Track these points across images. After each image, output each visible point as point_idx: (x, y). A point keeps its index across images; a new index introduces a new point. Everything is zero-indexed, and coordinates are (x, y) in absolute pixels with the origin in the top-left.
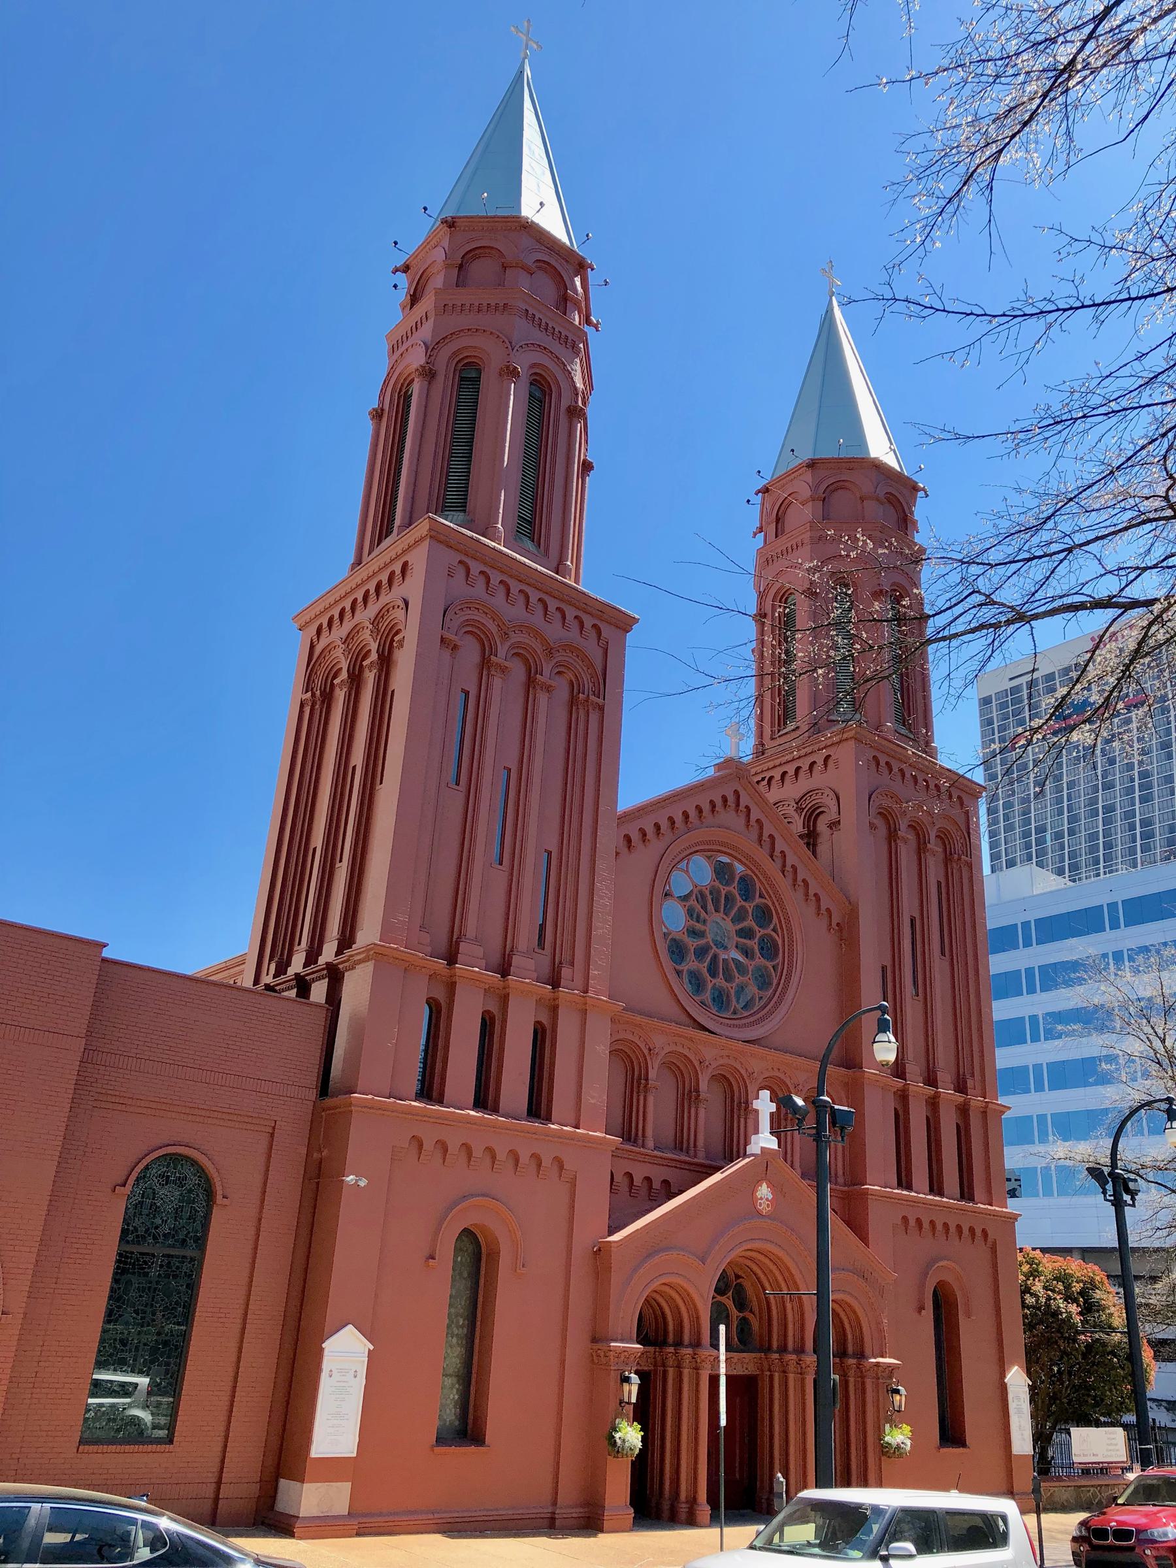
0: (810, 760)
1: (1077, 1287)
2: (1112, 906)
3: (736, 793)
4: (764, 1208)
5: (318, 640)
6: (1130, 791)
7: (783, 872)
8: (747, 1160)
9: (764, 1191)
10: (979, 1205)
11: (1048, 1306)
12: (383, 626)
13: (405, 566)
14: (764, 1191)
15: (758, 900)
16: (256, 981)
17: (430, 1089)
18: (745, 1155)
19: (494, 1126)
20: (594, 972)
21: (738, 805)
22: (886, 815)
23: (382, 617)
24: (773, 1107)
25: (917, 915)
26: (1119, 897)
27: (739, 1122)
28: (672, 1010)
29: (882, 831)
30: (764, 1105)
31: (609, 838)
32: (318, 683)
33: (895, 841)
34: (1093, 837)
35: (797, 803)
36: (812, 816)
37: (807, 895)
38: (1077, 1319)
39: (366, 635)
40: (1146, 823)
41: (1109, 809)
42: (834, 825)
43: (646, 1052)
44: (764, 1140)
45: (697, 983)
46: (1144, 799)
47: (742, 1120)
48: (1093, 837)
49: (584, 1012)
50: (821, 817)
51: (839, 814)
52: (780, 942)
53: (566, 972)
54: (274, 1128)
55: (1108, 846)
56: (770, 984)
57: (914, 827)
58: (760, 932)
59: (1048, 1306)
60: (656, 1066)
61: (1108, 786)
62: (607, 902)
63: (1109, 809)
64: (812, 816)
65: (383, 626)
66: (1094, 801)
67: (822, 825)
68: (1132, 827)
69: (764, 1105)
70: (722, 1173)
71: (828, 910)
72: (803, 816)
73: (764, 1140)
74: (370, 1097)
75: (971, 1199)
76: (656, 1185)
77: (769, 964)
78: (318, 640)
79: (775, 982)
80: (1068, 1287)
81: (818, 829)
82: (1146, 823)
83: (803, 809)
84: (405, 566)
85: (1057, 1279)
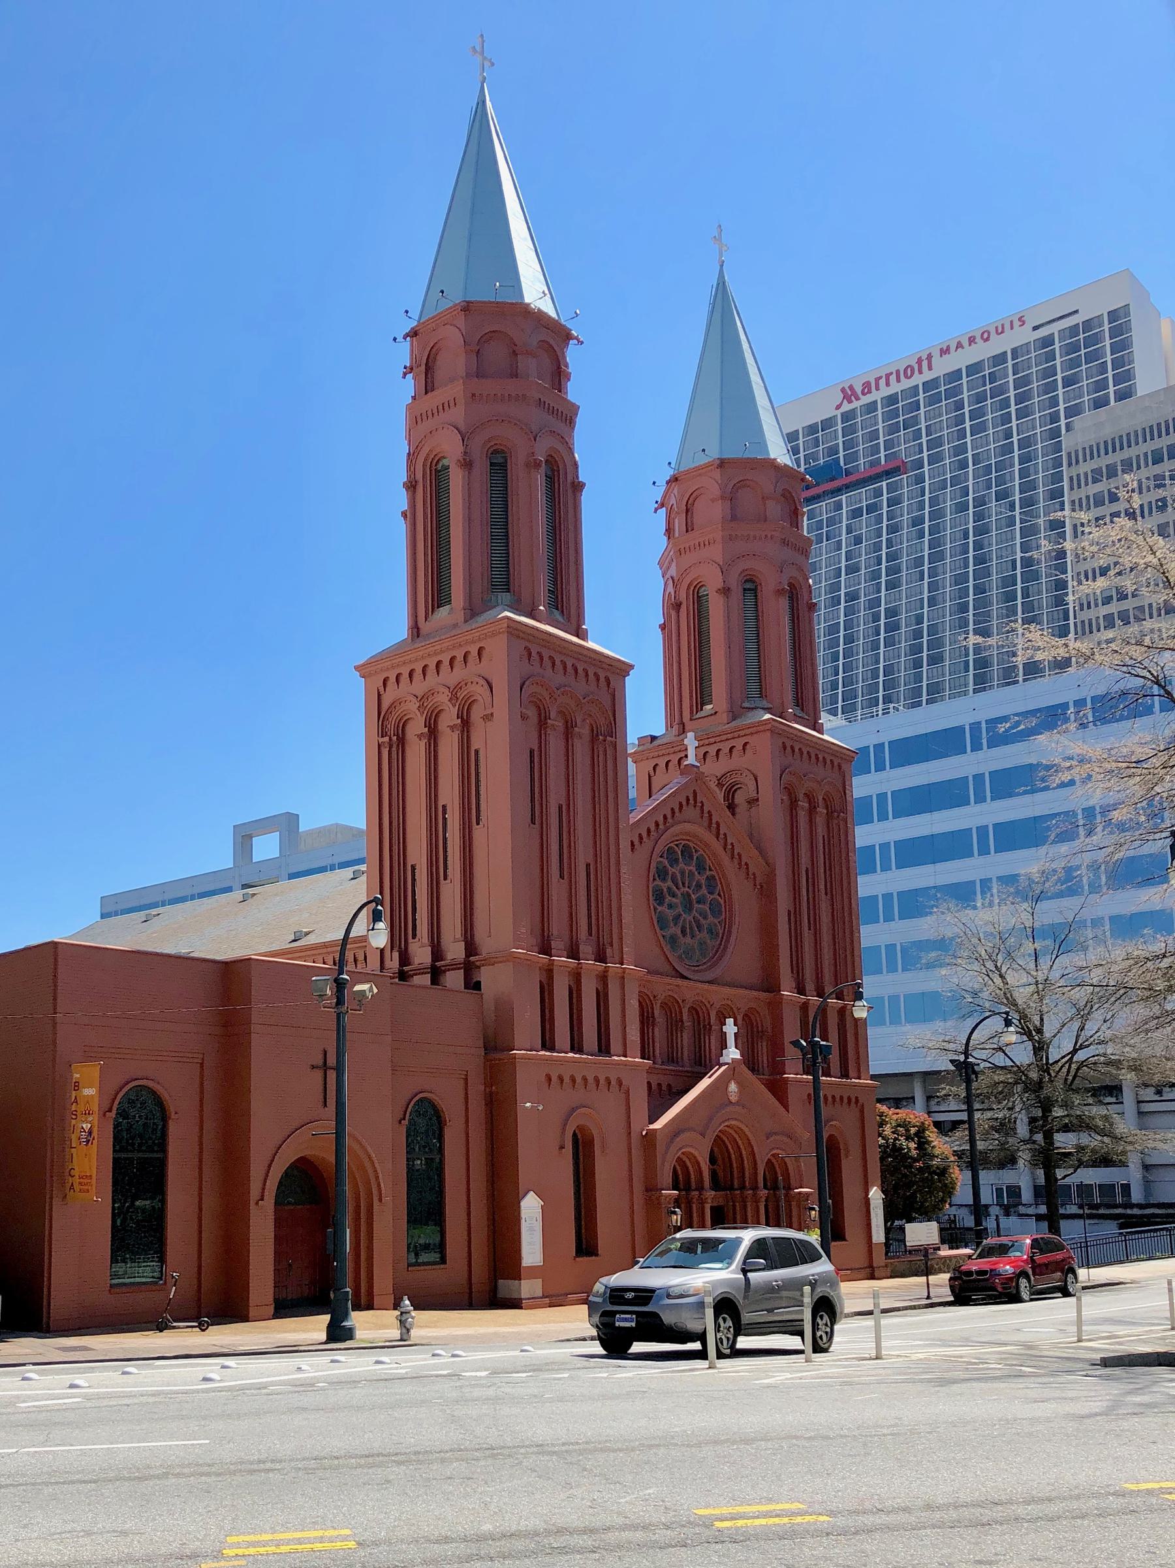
0: (729, 744)
1: (913, 1131)
2: (879, 747)
3: (695, 793)
4: (733, 1099)
5: (385, 690)
6: (876, 575)
7: (725, 849)
8: (723, 1068)
9: (733, 1087)
10: (853, 1080)
11: (894, 1144)
12: (461, 695)
13: (480, 651)
14: (733, 1087)
15: (708, 873)
16: (382, 967)
17: (548, 1043)
18: (721, 1065)
19: (585, 1062)
20: (625, 949)
21: (695, 802)
22: (790, 791)
23: (461, 688)
24: (735, 1029)
25: (810, 867)
26: (885, 738)
27: (704, 1038)
28: (667, 968)
29: (787, 802)
30: (730, 1028)
31: (624, 845)
32: (390, 727)
33: (795, 809)
34: (833, 629)
35: (718, 780)
36: (730, 793)
37: (740, 864)
38: (914, 1153)
39: (443, 698)
40: (892, 612)
41: (852, 597)
42: (752, 802)
43: (652, 998)
44: (733, 1053)
45: (673, 940)
46: (891, 585)
47: (707, 1037)
48: (833, 629)
49: (623, 978)
50: (738, 791)
51: (758, 793)
52: (722, 902)
53: (609, 951)
54: (467, 1075)
55: (849, 639)
56: (717, 934)
57: (809, 797)
58: (710, 897)
59: (894, 1144)
60: (658, 1005)
61: (852, 569)
62: (630, 897)
63: (852, 597)
64: (730, 793)
65: (461, 695)
66: (835, 587)
67: (740, 798)
68: (876, 618)
69: (730, 1028)
70: (710, 1077)
71: (754, 874)
72: (723, 791)
73: (733, 1053)
74: (523, 1052)
75: (847, 1076)
76: (664, 1088)
77: (716, 921)
78: (385, 690)
79: (721, 932)
80: (908, 1130)
81: (736, 801)
82: (892, 612)
83: (724, 785)
84: (480, 651)
85: (899, 1125)
